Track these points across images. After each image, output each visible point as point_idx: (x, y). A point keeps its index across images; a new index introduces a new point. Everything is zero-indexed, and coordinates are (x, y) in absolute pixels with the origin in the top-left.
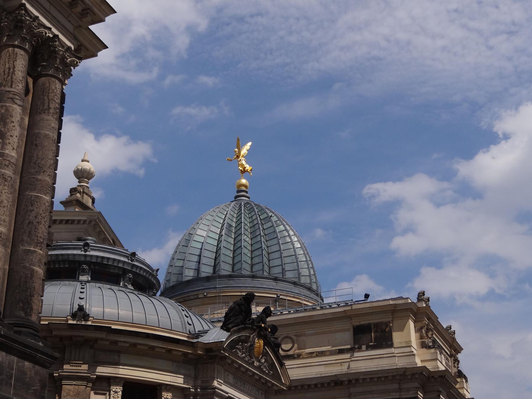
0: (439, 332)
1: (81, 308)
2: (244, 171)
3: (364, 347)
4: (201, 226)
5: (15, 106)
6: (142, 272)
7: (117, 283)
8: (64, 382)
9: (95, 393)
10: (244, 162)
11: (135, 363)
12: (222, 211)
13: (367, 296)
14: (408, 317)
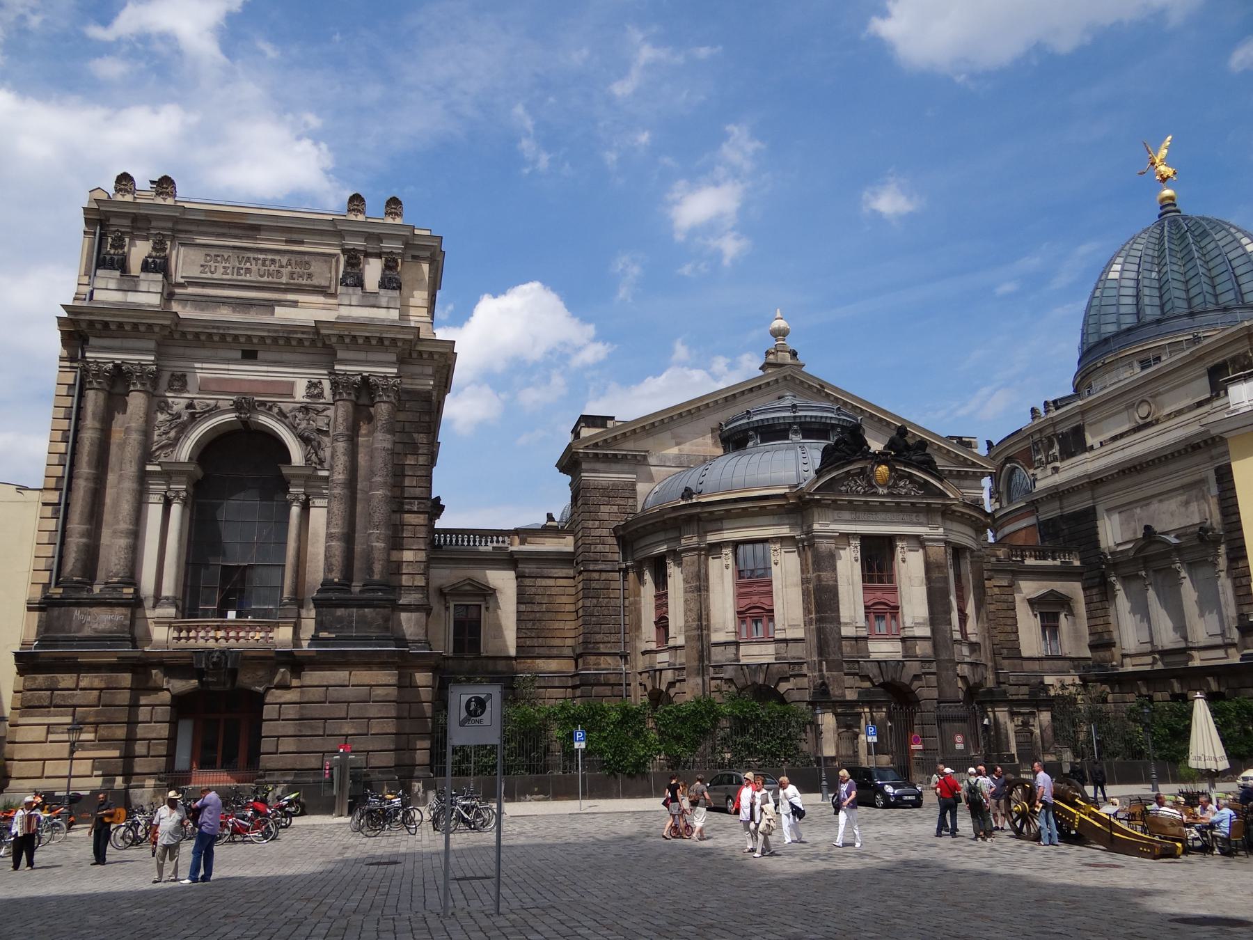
2: (1164, 179)
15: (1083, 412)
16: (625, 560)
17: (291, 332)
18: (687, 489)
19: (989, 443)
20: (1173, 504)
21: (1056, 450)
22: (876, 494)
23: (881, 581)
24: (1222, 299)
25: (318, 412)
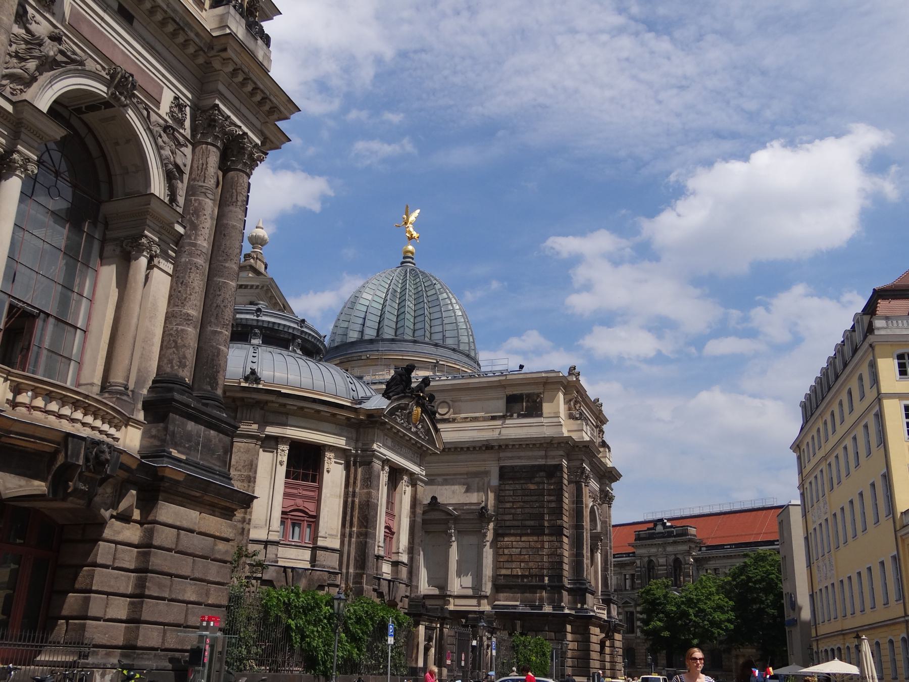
0: (587, 404)
1: (253, 372)
2: (411, 238)
3: (515, 415)
4: (367, 290)
5: (207, 200)
6: (310, 338)
7: (287, 348)
10: (411, 229)
12: (388, 276)
13: (521, 367)
14: (559, 390)
17: (188, 24)
25: (179, 145)
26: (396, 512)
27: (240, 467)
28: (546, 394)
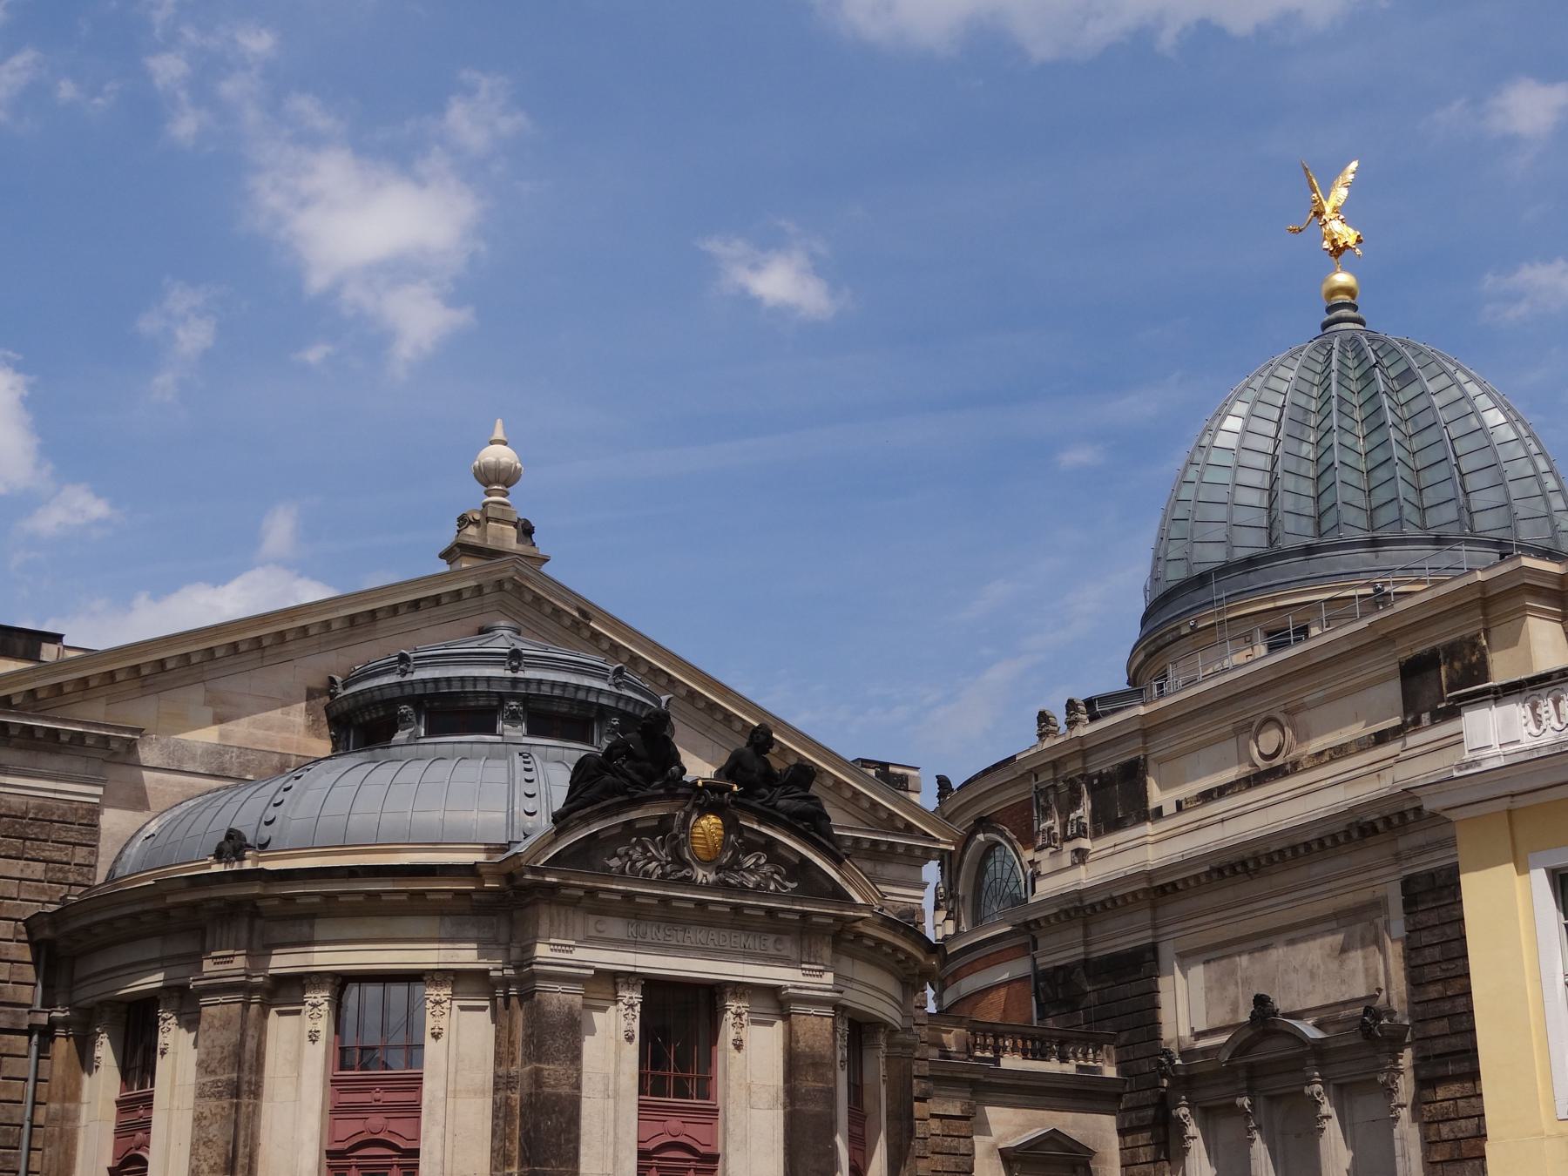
2: (1338, 250)
3: (1425, 717)
6: (546, 690)
7: (491, 730)
8: (204, 1000)
9: (280, 1013)
11: (349, 933)
14: (1523, 612)
15: (1147, 730)
16: (48, 1003)
18: (232, 835)
19: (943, 783)
20: (1315, 952)
21: (1084, 811)
22: (688, 882)
23: (682, 1092)
24: (1433, 518)
26: (720, 1105)
27: (214, 1065)
28: (1495, 632)
